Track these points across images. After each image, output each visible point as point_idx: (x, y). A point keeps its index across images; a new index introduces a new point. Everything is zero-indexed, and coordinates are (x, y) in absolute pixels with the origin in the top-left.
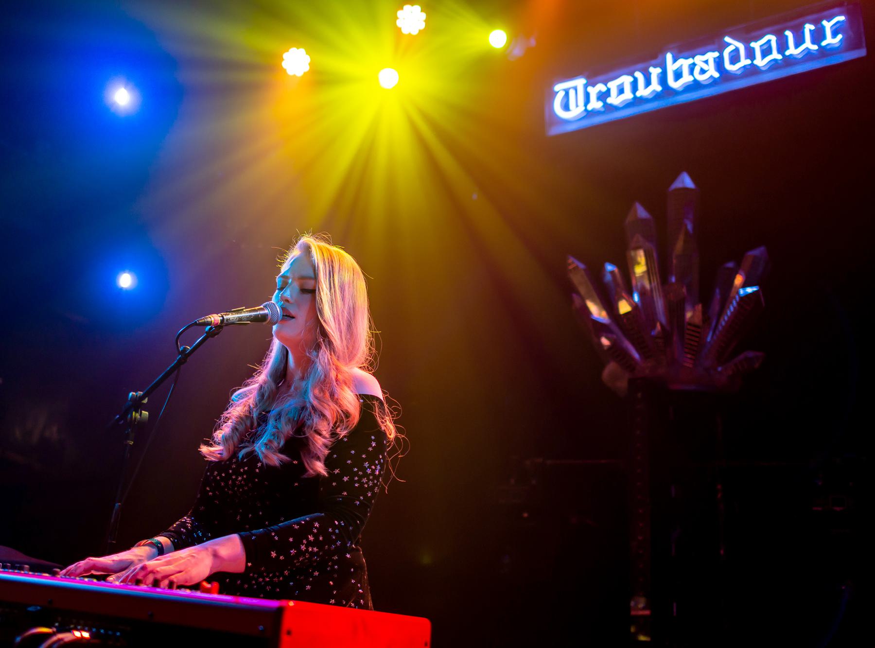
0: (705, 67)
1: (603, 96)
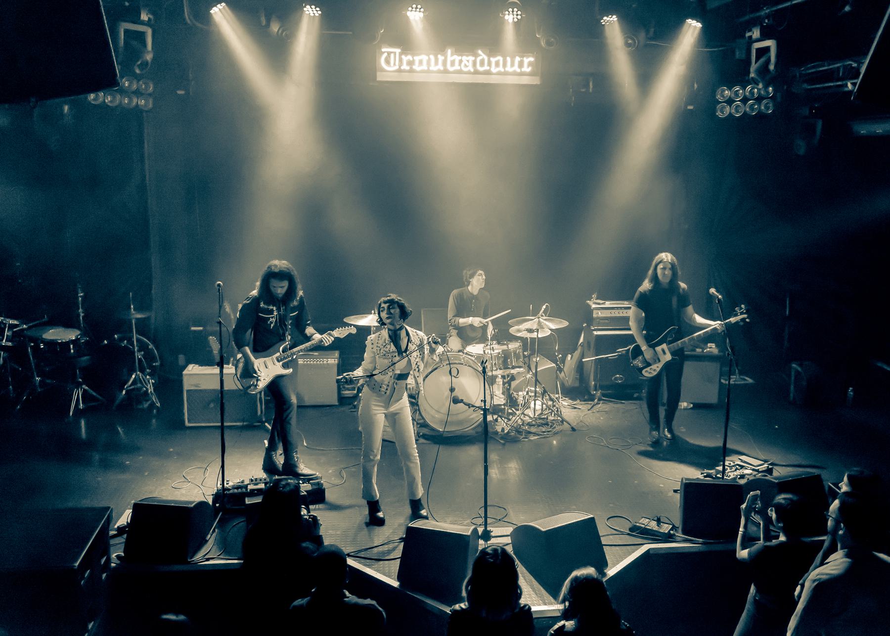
0: (467, 63)
1: (410, 63)
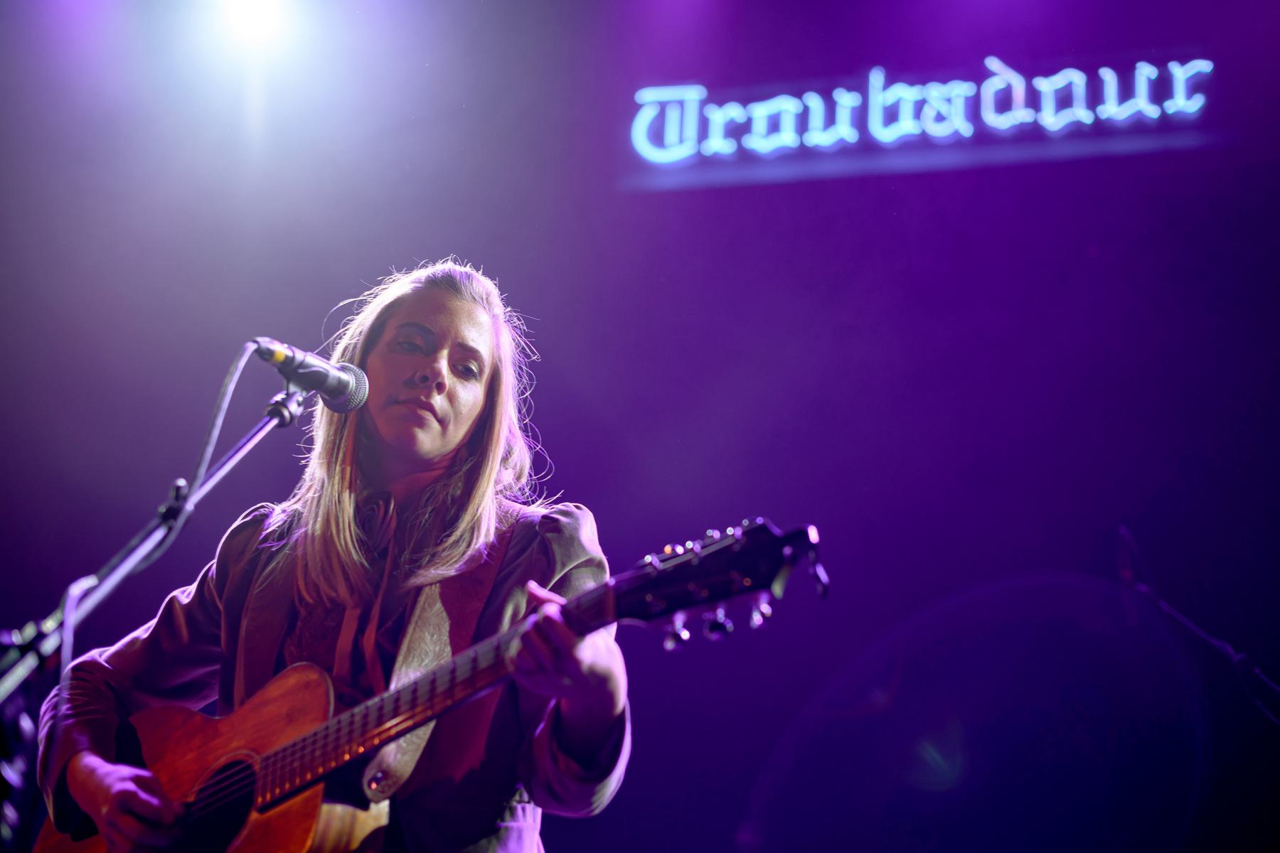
0: (944, 109)
